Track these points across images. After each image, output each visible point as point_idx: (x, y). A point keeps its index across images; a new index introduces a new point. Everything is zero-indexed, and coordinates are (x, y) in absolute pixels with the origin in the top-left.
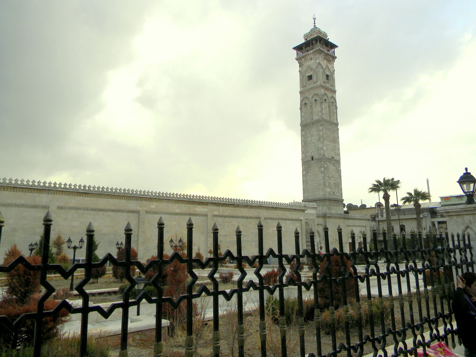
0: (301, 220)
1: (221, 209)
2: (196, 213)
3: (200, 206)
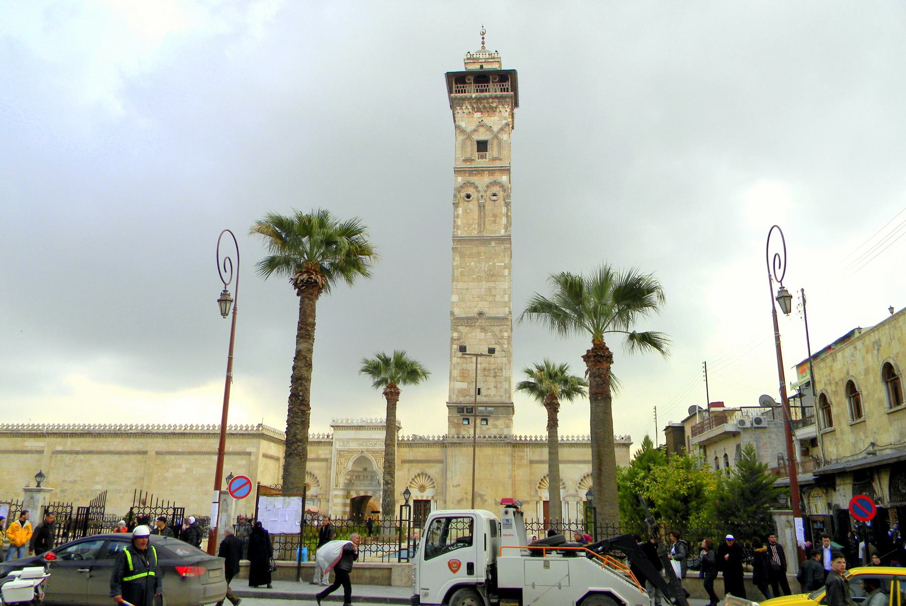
0: (249, 454)
2: (25, 449)
3: (32, 440)
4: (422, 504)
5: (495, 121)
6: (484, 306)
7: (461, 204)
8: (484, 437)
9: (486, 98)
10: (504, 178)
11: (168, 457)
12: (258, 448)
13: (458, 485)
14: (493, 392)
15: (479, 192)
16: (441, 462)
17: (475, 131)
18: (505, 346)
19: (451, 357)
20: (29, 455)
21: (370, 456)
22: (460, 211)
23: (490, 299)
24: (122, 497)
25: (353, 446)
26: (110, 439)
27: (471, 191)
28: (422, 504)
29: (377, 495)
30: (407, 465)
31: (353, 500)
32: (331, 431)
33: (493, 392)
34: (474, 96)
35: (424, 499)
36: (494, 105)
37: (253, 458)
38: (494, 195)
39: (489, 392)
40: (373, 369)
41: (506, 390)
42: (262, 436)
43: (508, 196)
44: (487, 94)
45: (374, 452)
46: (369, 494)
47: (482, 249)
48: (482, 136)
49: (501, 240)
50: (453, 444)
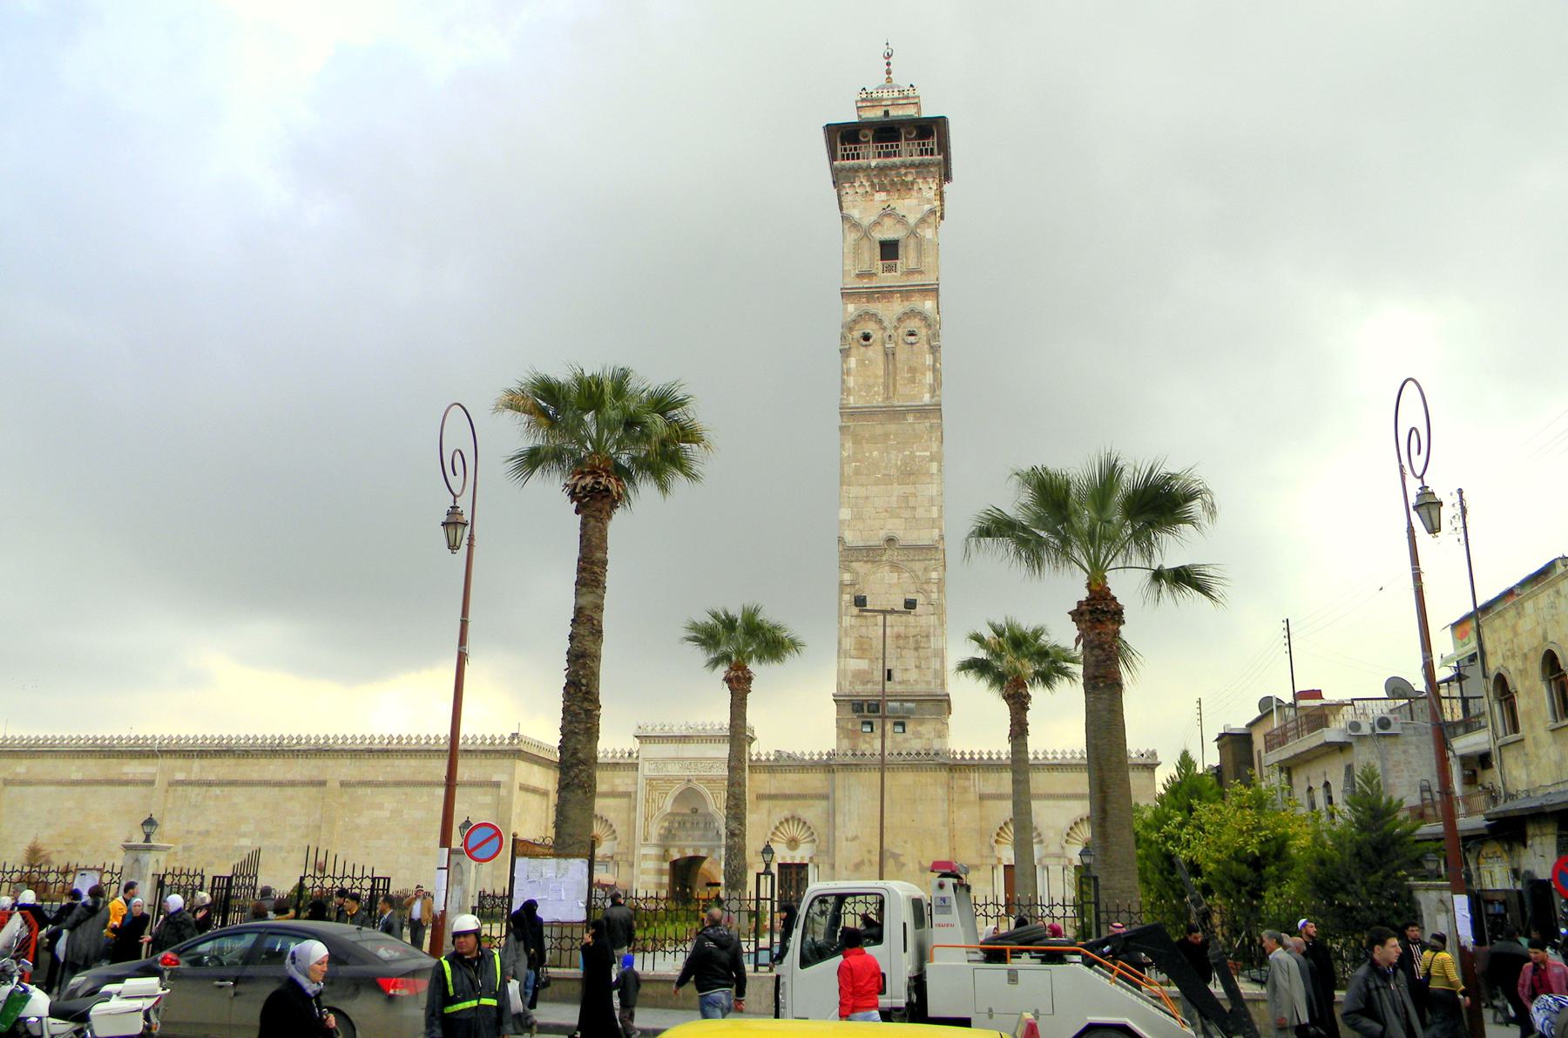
0: (497, 785)
1: (196, 764)
3: (136, 762)
4: (794, 871)
5: (911, 206)
6: (896, 527)
7: (854, 351)
8: (900, 754)
9: (894, 167)
10: (928, 305)
11: (361, 791)
12: (512, 775)
13: (855, 838)
14: (913, 675)
15: (884, 329)
16: (825, 797)
17: (877, 223)
19: (840, 617)
20: (130, 788)
21: (702, 788)
22: (852, 362)
23: (907, 514)
24: (284, 859)
25: (674, 770)
26: (263, 761)
27: (871, 327)
28: (794, 871)
29: (715, 856)
30: (766, 804)
31: (674, 864)
32: (634, 745)
33: (913, 675)
34: (873, 163)
36: (909, 178)
37: (503, 791)
38: (912, 334)
40: (707, 637)
41: (936, 672)
42: (517, 754)
43: (936, 336)
44: (896, 160)
45: (710, 781)
46: (702, 853)
47: (892, 427)
48: (889, 232)
49: (923, 412)
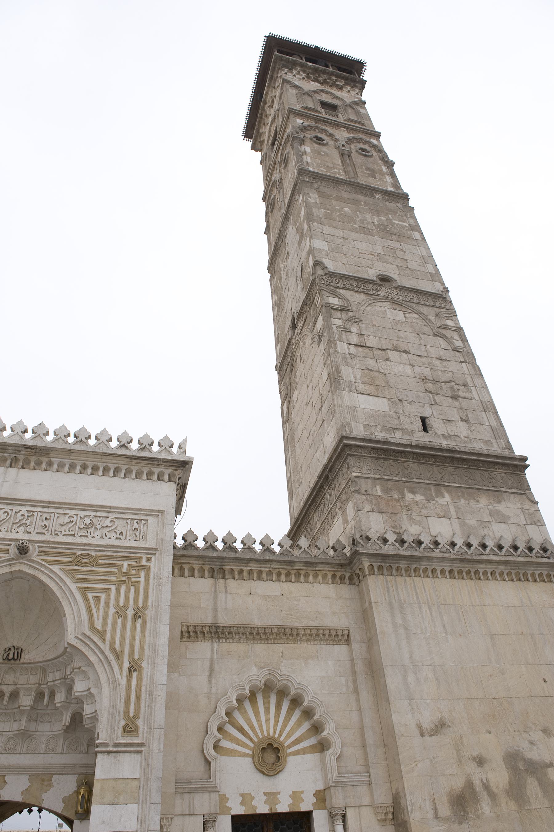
13: (440, 726)
14: (462, 430)
16: (340, 636)
18: (458, 344)
30: (203, 650)
33: (462, 430)
35: (283, 807)
39: (452, 430)
50: (387, 563)
